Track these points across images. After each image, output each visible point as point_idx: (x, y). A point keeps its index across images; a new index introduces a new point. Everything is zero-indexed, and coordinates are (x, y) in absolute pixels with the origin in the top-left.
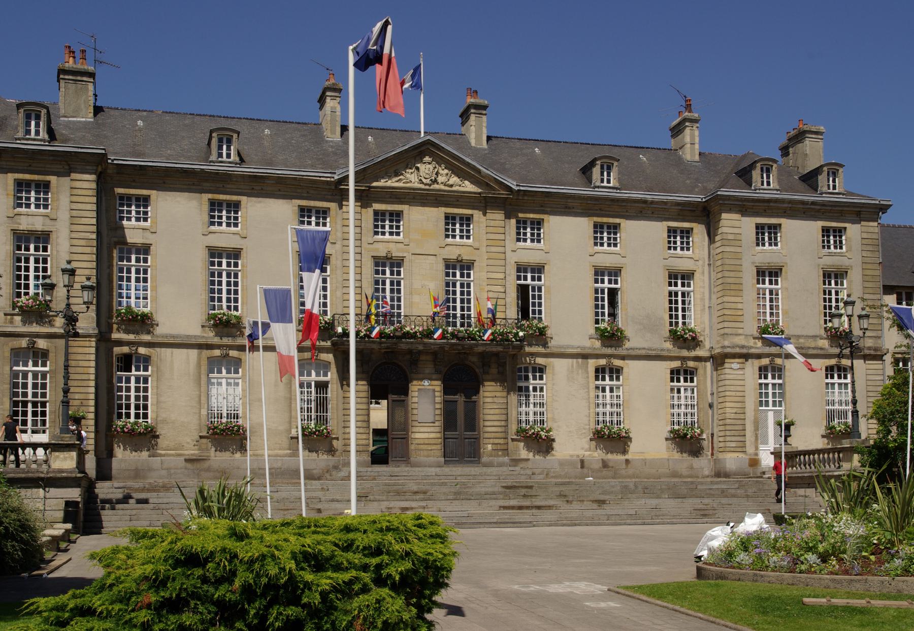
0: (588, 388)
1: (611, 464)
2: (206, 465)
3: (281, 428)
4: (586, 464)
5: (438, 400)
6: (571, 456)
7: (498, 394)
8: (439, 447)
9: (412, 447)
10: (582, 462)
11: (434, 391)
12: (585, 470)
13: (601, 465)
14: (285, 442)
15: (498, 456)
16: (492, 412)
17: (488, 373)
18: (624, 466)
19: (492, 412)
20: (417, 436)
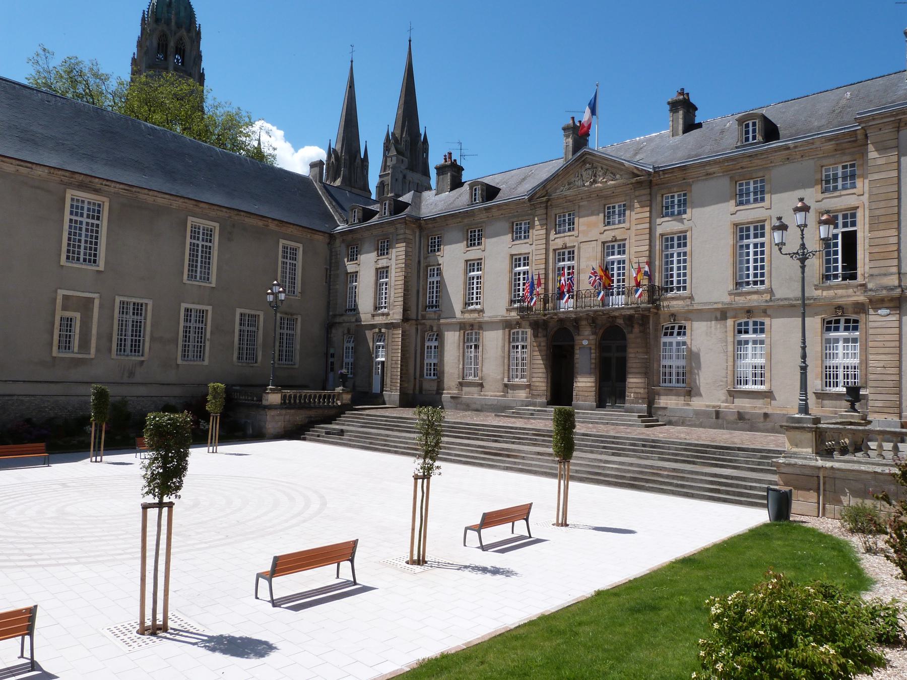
0: (726, 342)
1: (747, 417)
2: (460, 401)
3: (499, 377)
4: (721, 415)
5: (593, 355)
6: (708, 406)
7: (640, 350)
8: (593, 394)
9: (574, 394)
10: (718, 414)
11: (590, 349)
12: (720, 421)
13: (736, 416)
14: (501, 387)
15: (638, 403)
16: (634, 365)
17: (631, 332)
18: (762, 419)
19: (634, 365)
20: (579, 384)
